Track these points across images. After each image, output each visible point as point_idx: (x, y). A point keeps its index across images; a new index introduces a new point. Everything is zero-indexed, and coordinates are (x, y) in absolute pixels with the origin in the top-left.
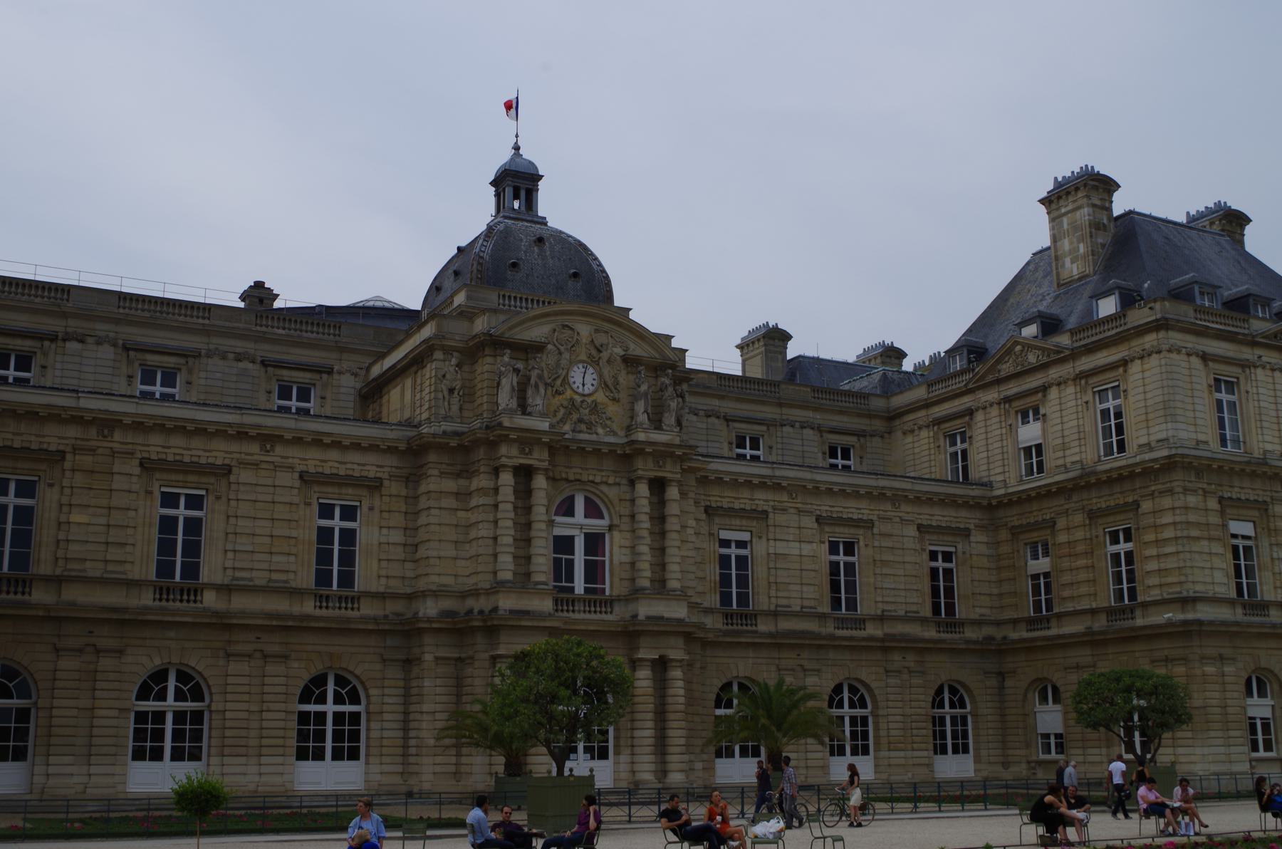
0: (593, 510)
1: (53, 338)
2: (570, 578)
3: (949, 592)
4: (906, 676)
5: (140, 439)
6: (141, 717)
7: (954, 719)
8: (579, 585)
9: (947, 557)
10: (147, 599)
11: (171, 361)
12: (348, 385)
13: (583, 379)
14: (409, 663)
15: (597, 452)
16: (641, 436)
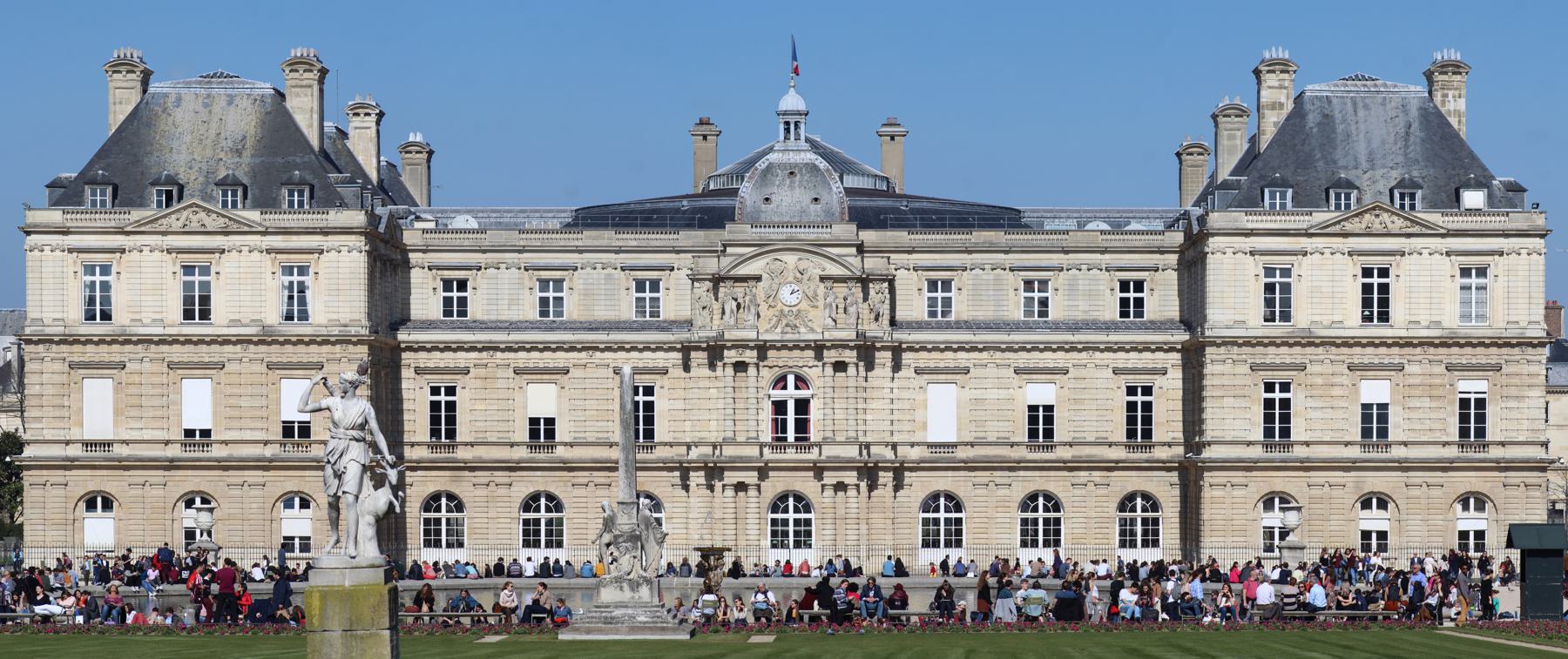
0: (801, 382)
1: (479, 269)
2: (784, 430)
3: (1147, 420)
4: (1091, 487)
5: (512, 355)
6: (526, 522)
7: (1145, 521)
8: (791, 435)
9: (1147, 391)
10: (522, 453)
11: (557, 274)
12: (681, 276)
13: (787, 296)
14: (686, 488)
15: (796, 347)
16: (827, 336)
